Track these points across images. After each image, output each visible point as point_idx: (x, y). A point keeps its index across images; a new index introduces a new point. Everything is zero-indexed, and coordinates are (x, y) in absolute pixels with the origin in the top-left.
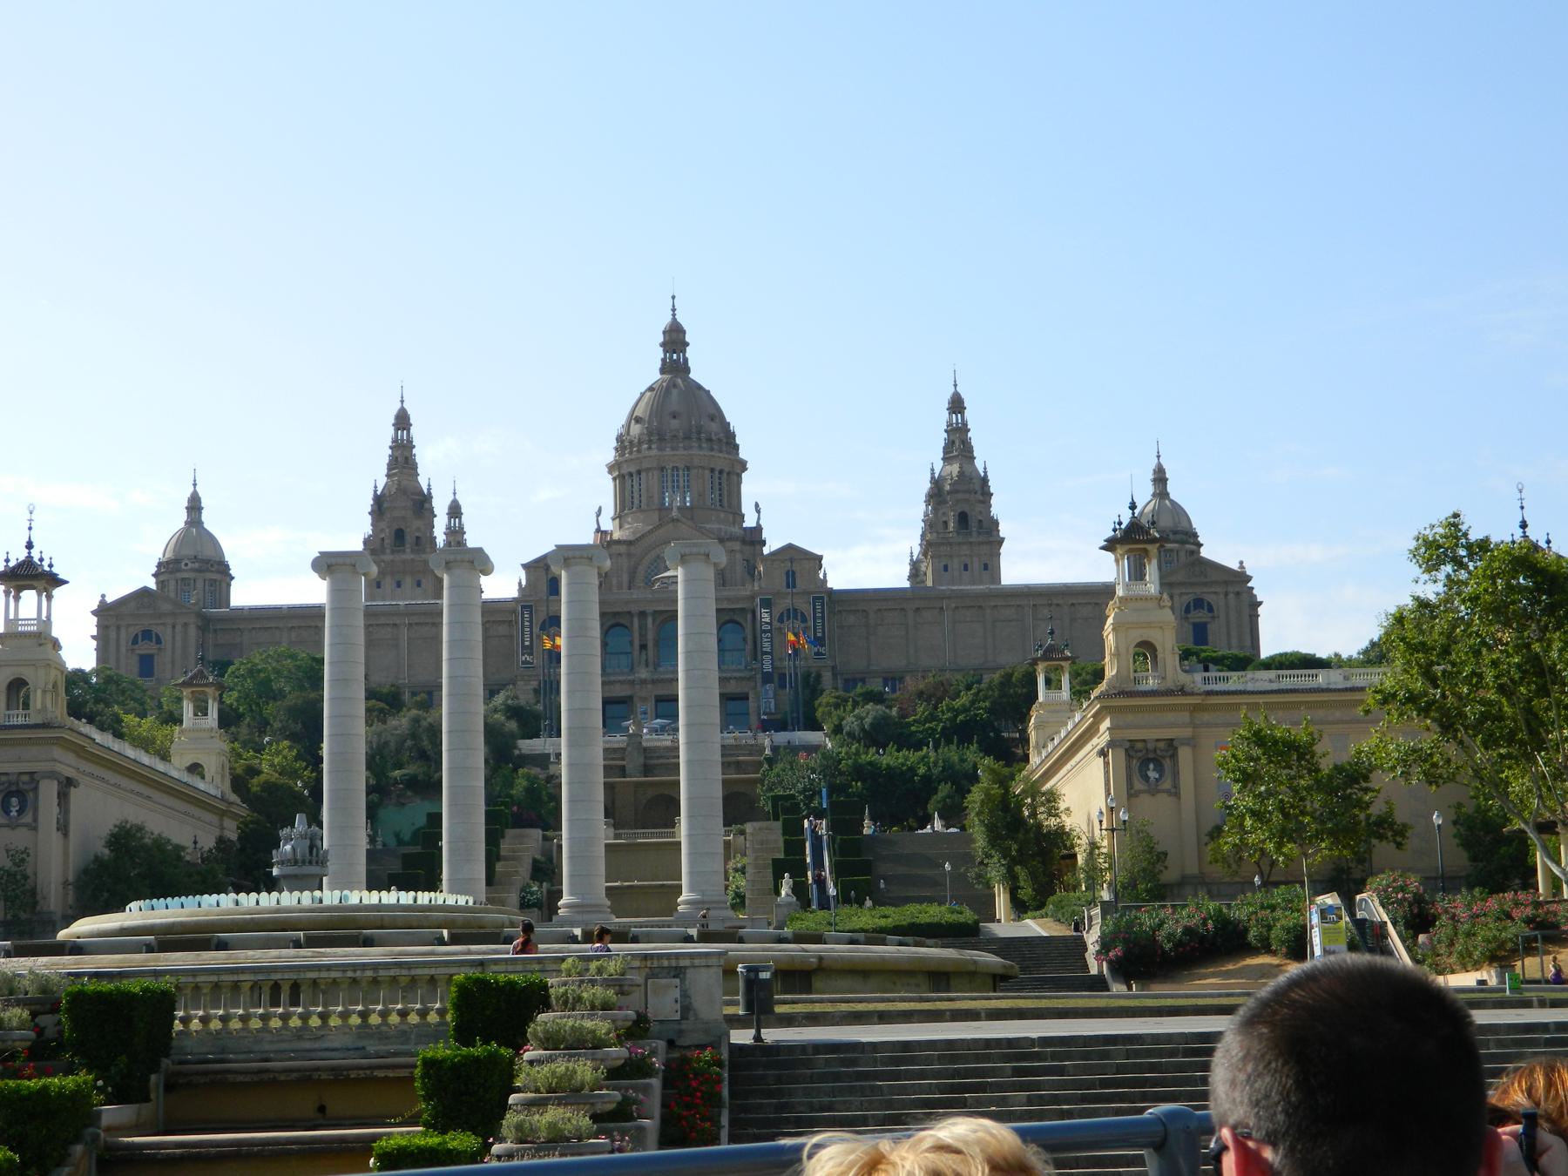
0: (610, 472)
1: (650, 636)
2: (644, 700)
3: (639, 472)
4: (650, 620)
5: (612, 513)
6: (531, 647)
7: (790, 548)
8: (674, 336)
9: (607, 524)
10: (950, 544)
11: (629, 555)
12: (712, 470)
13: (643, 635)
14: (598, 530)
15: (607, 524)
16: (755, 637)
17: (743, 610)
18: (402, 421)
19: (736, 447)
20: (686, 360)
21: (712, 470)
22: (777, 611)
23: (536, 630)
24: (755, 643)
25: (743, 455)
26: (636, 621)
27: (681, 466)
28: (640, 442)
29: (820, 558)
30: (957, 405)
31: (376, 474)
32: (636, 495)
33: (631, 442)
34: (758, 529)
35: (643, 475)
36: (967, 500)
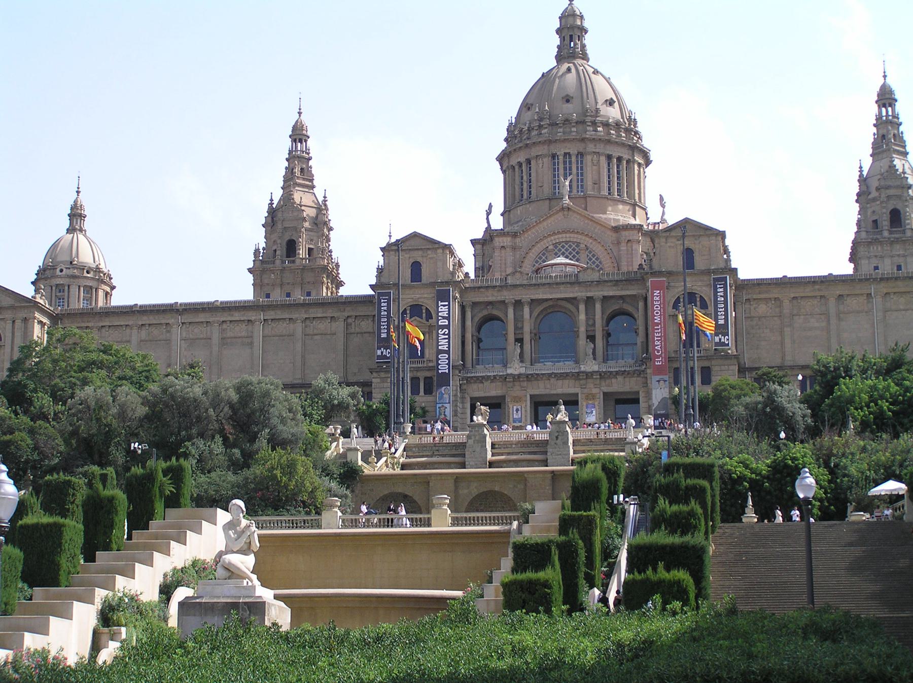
0: (502, 169)
1: (527, 328)
2: (517, 399)
3: (529, 162)
4: (526, 310)
5: (502, 210)
9: (497, 223)
10: (881, 243)
12: (609, 157)
13: (518, 328)
14: (488, 229)
15: (497, 223)
17: (634, 296)
18: (299, 135)
20: (583, 46)
25: (646, 143)
26: (511, 311)
27: (573, 151)
28: (530, 130)
29: (722, 235)
30: (886, 98)
31: (272, 187)
32: (525, 185)
33: (521, 131)
34: (663, 221)
36: (899, 197)
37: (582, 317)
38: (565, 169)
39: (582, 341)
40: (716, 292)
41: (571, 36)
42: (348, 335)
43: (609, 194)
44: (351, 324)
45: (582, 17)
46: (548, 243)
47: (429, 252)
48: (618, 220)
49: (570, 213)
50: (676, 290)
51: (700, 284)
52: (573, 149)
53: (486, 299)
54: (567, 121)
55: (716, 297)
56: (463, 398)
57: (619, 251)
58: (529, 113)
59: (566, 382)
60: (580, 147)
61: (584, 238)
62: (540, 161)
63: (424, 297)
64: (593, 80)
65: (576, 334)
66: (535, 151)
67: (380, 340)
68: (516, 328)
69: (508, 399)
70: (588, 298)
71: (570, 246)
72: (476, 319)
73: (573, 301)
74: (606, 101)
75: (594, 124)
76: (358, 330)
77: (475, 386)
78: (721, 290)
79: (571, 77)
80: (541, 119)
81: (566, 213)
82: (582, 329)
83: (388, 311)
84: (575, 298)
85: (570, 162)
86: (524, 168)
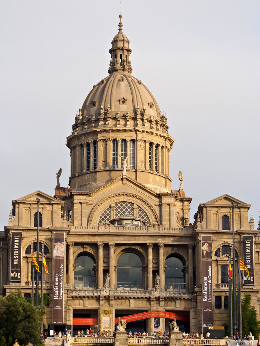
2: (106, 312)
3: (95, 143)
4: (112, 250)
6: (19, 266)
7: (227, 198)
8: (120, 45)
9: (65, 183)
11: (87, 204)
12: (151, 144)
16: (194, 268)
19: (167, 128)
20: (129, 63)
21: (151, 144)
22: (215, 246)
23: (23, 254)
24: (194, 273)
37: (151, 257)
38: (122, 150)
39: (151, 275)
40: (245, 246)
41: (121, 55)
43: (150, 170)
45: (128, 42)
46: (112, 202)
47: (47, 206)
48: (157, 188)
49: (127, 182)
50: (218, 244)
52: (129, 136)
53: (84, 241)
54: (125, 117)
55: (245, 249)
56: (69, 310)
57: (161, 211)
59: (141, 302)
60: (133, 136)
61: (136, 200)
63: (43, 237)
64: (139, 88)
65: (145, 269)
66: (100, 136)
67: (13, 266)
68: (104, 262)
69: (101, 312)
70: (154, 244)
71: (127, 205)
72: (76, 255)
73: (144, 246)
74: (149, 104)
75: (142, 120)
77: (77, 302)
78: (249, 245)
79: (124, 84)
80: (105, 114)
81: (124, 182)
82: (151, 266)
83: (20, 246)
84: (146, 244)
85: (126, 146)
86: (91, 148)
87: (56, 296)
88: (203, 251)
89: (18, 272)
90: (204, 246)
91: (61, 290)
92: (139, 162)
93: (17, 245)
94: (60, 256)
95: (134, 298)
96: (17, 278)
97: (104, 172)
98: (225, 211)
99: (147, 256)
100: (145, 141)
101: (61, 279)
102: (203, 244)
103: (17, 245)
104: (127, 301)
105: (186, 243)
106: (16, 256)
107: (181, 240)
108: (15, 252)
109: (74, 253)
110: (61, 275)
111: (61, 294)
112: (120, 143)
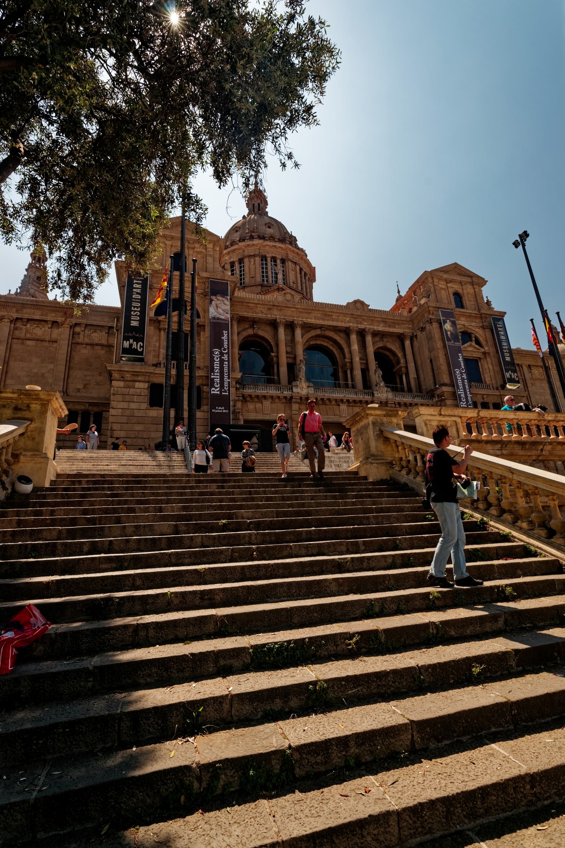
3: (241, 261)
4: (298, 332)
26: (281, 331)
35: (246, 260)
37: (355, 347)
41: (259, 204)
42: (73, 344)
44: (79, 334)
51: (474, 324)
58: (238, 233)
62: (252, 260)
72: (242, 337)
76: (87, 340)
77: (251, 406)
82: (357, 359)
84: (348, 328)
86: (237, 266)
87: (216, 388)
88: (446, 330)
89: (137, 340)
90: (446, 325)
91: (226, 377)
92: (291, 281)
93: (138, 293)
94: (223, 317)
95: (348, 401)
96: (135, 352)
97: (254, 287)
98: (456, 287)
99: (349, 345)
100: (295, 263)
101: (225, 357)
102: (445, 322)
103: (138, 293)
104: (336, 407)
105: (401, 331)
106: (135, 311)
107: (395, 327)
108: (134, 304)
109: (238, 334)
110: (225, 350)
111: (226, 384)
112: (269, 260)
